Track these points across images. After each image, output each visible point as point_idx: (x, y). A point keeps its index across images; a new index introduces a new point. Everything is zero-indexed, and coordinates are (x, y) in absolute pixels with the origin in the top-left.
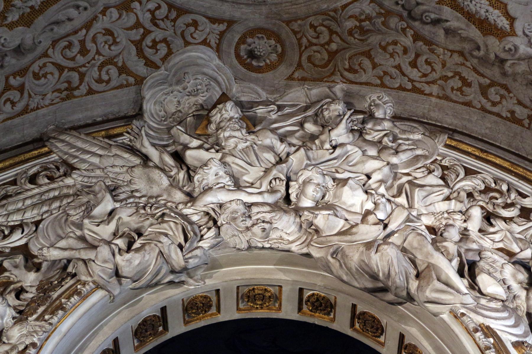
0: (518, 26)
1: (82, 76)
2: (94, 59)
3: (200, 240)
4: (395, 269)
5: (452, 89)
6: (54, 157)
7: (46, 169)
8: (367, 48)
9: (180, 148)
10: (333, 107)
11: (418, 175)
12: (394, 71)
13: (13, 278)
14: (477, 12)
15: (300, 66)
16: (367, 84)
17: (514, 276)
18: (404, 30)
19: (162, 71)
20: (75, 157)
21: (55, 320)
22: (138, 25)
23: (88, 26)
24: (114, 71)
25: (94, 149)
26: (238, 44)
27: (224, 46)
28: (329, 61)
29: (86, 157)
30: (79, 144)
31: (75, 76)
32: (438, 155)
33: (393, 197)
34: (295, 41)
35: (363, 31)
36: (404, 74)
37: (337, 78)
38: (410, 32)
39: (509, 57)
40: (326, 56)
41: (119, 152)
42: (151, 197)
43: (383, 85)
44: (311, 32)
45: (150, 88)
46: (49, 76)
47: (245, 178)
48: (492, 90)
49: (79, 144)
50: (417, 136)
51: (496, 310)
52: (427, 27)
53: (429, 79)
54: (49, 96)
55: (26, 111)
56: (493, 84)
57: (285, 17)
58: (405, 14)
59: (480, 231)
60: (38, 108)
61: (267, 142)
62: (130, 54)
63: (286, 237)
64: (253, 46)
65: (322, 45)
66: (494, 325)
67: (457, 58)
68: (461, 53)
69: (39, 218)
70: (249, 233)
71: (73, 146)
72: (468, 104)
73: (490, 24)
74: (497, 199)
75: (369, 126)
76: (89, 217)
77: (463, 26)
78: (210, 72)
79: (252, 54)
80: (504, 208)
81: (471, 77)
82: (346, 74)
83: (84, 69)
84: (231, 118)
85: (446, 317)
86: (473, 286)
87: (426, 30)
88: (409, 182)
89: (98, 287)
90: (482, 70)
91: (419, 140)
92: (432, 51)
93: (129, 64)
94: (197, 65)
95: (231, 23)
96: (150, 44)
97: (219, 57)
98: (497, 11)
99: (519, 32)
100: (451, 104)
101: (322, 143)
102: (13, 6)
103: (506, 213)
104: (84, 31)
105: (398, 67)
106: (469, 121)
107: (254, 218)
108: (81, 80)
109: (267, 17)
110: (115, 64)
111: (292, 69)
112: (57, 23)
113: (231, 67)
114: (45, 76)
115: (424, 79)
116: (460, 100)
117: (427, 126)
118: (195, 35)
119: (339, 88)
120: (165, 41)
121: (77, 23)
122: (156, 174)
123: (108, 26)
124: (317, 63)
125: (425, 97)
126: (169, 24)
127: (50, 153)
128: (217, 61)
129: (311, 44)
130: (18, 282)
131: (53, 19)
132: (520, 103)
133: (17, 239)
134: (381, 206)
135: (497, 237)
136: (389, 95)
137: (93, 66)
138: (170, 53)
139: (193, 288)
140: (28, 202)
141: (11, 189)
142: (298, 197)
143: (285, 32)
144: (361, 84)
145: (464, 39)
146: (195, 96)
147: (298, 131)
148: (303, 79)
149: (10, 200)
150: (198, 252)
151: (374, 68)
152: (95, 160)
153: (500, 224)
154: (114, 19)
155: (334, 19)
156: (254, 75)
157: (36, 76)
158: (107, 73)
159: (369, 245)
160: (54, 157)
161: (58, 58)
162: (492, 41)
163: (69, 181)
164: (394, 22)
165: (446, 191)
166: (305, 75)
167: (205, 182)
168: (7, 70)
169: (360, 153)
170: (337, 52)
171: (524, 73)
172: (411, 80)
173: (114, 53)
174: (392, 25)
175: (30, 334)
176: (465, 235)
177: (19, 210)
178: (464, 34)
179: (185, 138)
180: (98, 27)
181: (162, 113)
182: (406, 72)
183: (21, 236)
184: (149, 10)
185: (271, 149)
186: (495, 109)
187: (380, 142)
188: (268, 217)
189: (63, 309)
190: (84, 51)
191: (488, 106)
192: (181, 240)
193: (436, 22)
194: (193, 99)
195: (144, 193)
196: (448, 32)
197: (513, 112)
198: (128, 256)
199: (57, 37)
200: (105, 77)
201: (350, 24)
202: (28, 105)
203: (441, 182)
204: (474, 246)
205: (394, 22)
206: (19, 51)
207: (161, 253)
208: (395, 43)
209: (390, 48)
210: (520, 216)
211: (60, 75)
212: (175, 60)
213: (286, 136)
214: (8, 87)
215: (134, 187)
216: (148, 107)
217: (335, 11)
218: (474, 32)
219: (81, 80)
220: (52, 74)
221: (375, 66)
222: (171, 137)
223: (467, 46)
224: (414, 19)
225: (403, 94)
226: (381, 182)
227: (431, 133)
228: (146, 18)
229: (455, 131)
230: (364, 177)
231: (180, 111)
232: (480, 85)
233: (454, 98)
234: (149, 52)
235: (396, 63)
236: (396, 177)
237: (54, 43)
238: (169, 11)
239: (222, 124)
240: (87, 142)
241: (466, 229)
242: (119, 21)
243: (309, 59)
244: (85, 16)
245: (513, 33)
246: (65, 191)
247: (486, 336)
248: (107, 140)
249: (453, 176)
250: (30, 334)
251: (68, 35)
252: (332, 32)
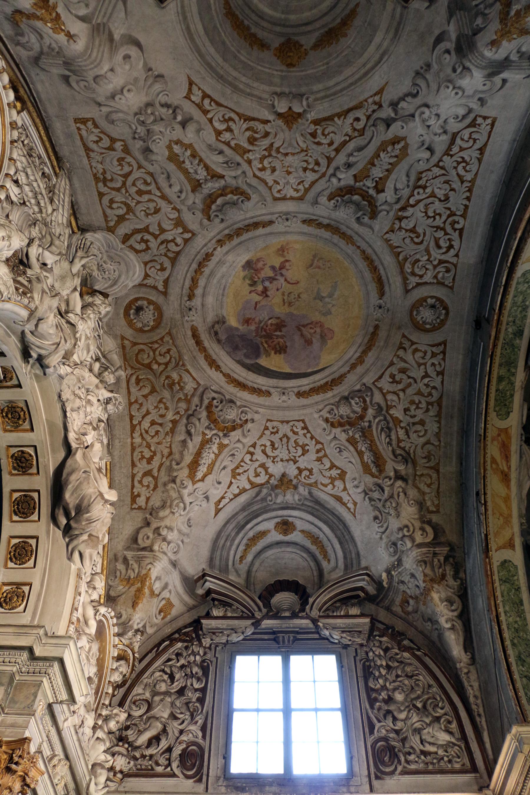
0: (200, 484)
1: (118, 190)
2: (133, 199)
5: (142, 452)
8: (158, 389)
12: (144, 410)
14: (202, 458)
15: (135, 344)
16: (129, 392)
18: (178, 413)
19: (120, 246)
22: (163, 231)
23: (164, 197)
24: (121, 212)
26: (147, 299)
27: (144, 289)
28: (143, 365)
31: (119, 185)
34: (155, 339)
35: (171, 386)
36: (143, 417)
37: (129, 371)
38: (177, 417)
39: (178, 484)
40: (146, 362)
43: (131, 404)
44: (164, 350)
45: (105, 238)
46: (120, 168)
48: (150, 479)
52: (184, 428)
53: (145, 435)
54: (100, 166)
55: (88, 149)
56: (155, 479)
57: (174, 331)
58: (190, 412)
60: (88, 157)
62: (137, 224)
64: (147, 310)
65: (154, 359)
67: (166, 451)
68: (171, 453)
70: (72, 397)
72: (133, 465)
73: (196, 468)
77: (190, 451)
78: (121, 281)
79: (139, 309)
81: (156, 462)
82: (134, 377)
83: (123, 191)
84: (100, 313)
87: (181, 428)
90: (163, 469)
92: (167, 434)
93: (127, 223)
94: (128, 271)
95: (165, 294)
96: (145, 238)
97: (134, 286)
98: (205, 469)
99: (195, 487)
100: (129, 453)
102: (186, 149)
104: (159, 194)
105: (148, 413)
106: (121, 467)
108: (113, 189)
109: (172, 319)
110: (127, 213)
111: (131, 339)
112: (168, 177)
113: (127, 295)
114: (120, 165)
115: (143, 431)
116: (135, 459)
118: (153, 269)
119: (122, 373)
120: (148, 248)
121: (167, 191)
123: (163, 210)
124: (140, 356)
125: (129, 433)
126: (163, 252)
128: (131, 285)
129: (154, 351)
131: (172, 175)
132: (148, 499)
136: (124, 410)
137: (127, 198)
138: (137, 251)
143: (161, 332)
144: (128, 388)
145: (181, 453)
146: (98, 269)
148: (123, 347)
151: (143, 396)
154: (169, 215)
155: (177, 365)
156: (122, 311)
157: (120, 160)
158: (119, 208)
161: (136, 174)
162: (186, 472)
164: (183, 405)
166: (128, 348)
168: (130, 142)
170: (151, 369)
171: (170, 497)
172: (140, 423)
173: (138, 214)
174: (180, 405)
178: (185, 452)
180: (162, 204)
182: (145, 419)
183: (17, 193)
184: (175, 239)
186: (136, 483)
190: (140, 193)
191: (137, 478)
193: (189, 433)
194: (95, 268)
196: (184, 442)
197: (139, 495)
199: (156, 176)
200: (115, 206)
201: (175, 376)
202: (93, 151)
205: (183, 405)
206: (147, 151)
208: (167, 408)
209: (162, 405)
211: (120, 175)
212: (132, 256)
214: (113, 140)
217: (183, 365)
218: (188, 459)
219: (113, 189)
220: (122, 169)
221: (145, 396)
223: (177, 456)
224: (188, 419)
225: (128, 419)
232: (151, 470)
233: (135, 454)
234: (138, 237)
235: (151, 411)
237: (151, 175)
238: (174, 252)
242: (166, 219)
243: (141, 351)
244: (173, 197)
245: (194, 483)
251: (156, 183)
252: (167, 364)
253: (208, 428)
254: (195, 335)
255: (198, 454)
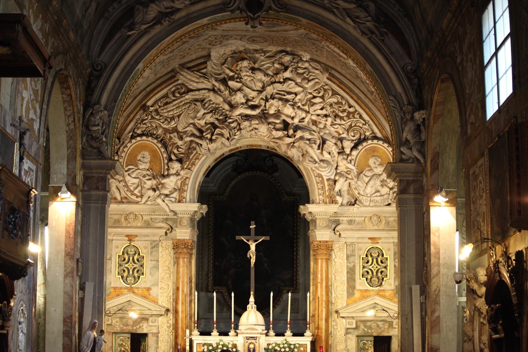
3: (235, 135)
4: (295, 157)
6: (180, 82)
7: (178, 89)
9: (226, 76)
10: (286, 58)
11: (315, 94)
13: (175, 142)
17: (335, 150)
20: (188, 83)
21: (192, 169)
25: (194, 79)
29: (191, 83)
30: (189, 77)
32: (324, 83)
33: (303, 105)
41: (203, 81)
42: (216, 104)
47: (251, 95)
49: (189, 77)
50: (317, 72)
51: (325, 168)
59: (332, 122)
61: (259, 77)
63: (263, 134)
66: (323, 174)
69: (178, 114)
70: (251, 133)
71: (186, 78)
74: (340, 107)
75: (300, 65)
76: (195, 117)
79: (254, 40)
80: (342, 112)
84: (246, 67)
85: (309, 168)
86: (322, 153)
88: (309, 100)
89: (203, 155)
91: (318, 74)
101: (280, 78)
103: (341, 114)
107: (253, 126)
117: (323, 65)
122: (218, 97)
127: (178, 80)
130: (177, 143)
133: (173, 124)
134: (297, 116)
135: (336, 127)
139: (232, 147)
140: (175, 107)
141: (168, 100)
142: (269, 108)
147: (270, 67)
149: (168, 106)
150: (234, 141)
152: (195, 84)
153: (338, 121)
159: (288, 145)
160: (180, 82)
163: (187, 97)
165: (322, 105)
167: (236, 100)
169: (294, 83)
175: (187, 174)
176: (325, 127)
177: (172, 110)
179: (228, 71)
181: (218, 56)
185: (260, 81)
187: (303, 74)
188: (257, 126)
189: (194, 165)
190: (189, 49)
192: (229, 136)
195: (214, 101)
198: (212, 145)
203: (321, 100)
204: (327, 132)
207: (222, 143)
210: (347, 116)
213: (267, 70)
214: (164, 65)
215: (210, 99)
216: (213, 54)
222: (222, 69)
226: (299, 100)
227: (323, 70)
228: (213, 39)
229: (333, 68)
230: (294, 95)
231: (225, 54)
236: (306, 95)
239: (242, 69)
240: (191, 75)
241: (326, 124)
246: (186, 101)
247: (319, 177)
248: (198, 73)
249: (327, 95)
250: (187, 174)
253: (321, 43)
254: (270, 31)
255: (334, 51)
